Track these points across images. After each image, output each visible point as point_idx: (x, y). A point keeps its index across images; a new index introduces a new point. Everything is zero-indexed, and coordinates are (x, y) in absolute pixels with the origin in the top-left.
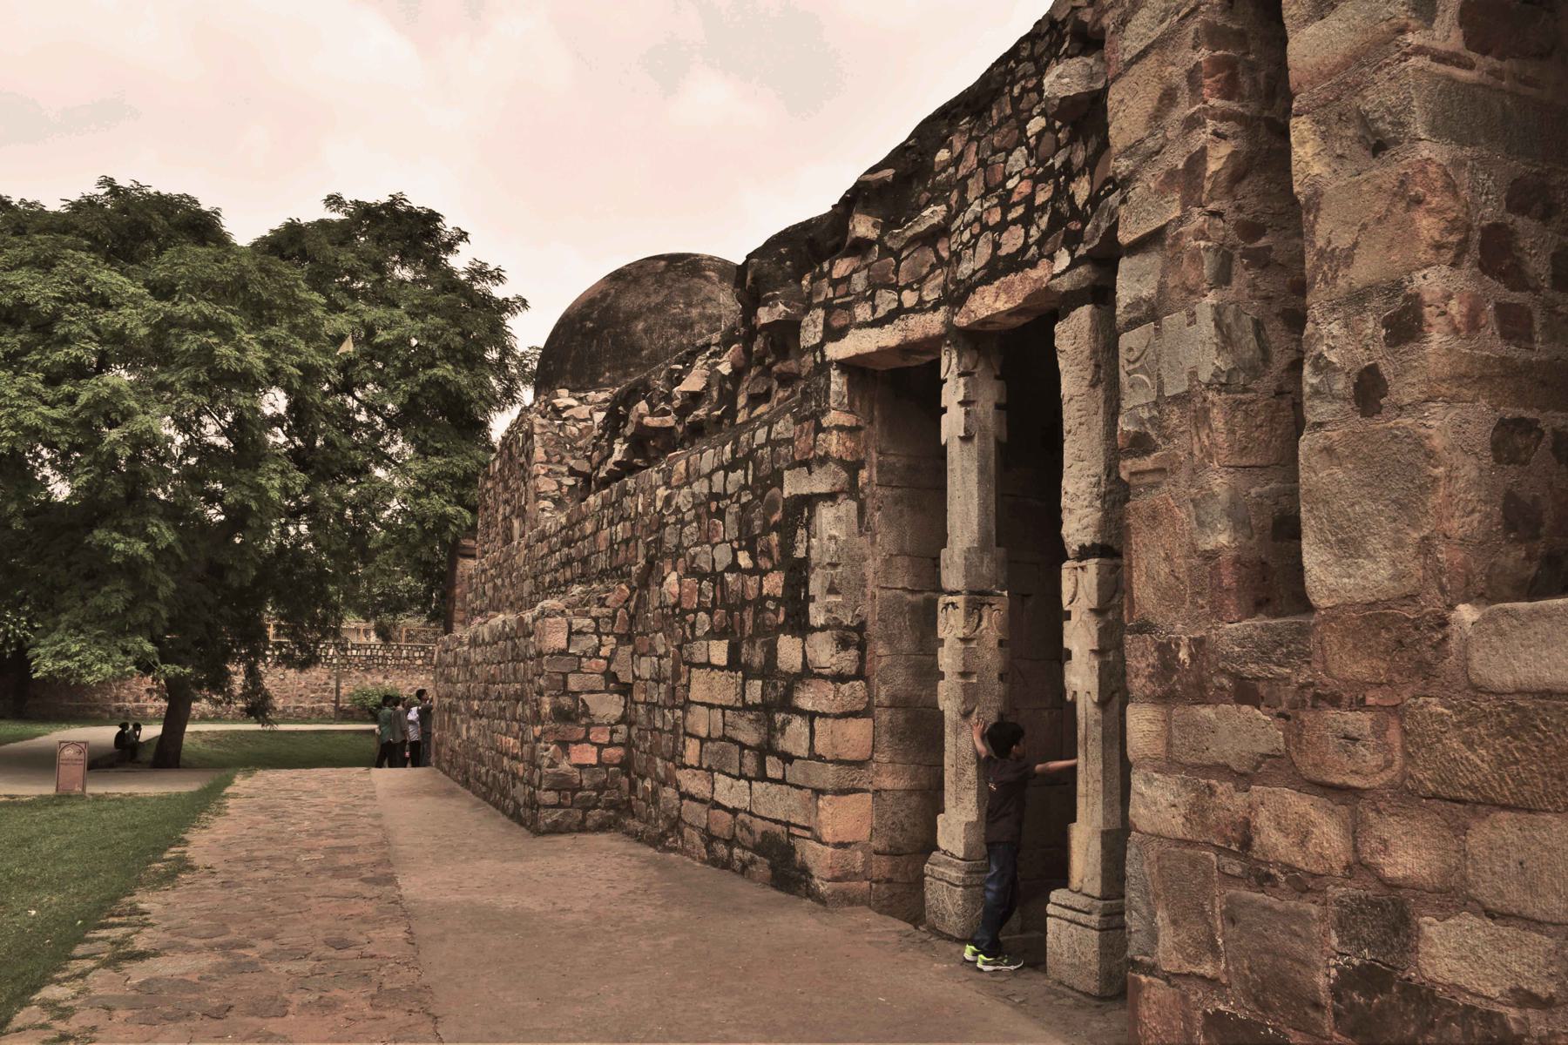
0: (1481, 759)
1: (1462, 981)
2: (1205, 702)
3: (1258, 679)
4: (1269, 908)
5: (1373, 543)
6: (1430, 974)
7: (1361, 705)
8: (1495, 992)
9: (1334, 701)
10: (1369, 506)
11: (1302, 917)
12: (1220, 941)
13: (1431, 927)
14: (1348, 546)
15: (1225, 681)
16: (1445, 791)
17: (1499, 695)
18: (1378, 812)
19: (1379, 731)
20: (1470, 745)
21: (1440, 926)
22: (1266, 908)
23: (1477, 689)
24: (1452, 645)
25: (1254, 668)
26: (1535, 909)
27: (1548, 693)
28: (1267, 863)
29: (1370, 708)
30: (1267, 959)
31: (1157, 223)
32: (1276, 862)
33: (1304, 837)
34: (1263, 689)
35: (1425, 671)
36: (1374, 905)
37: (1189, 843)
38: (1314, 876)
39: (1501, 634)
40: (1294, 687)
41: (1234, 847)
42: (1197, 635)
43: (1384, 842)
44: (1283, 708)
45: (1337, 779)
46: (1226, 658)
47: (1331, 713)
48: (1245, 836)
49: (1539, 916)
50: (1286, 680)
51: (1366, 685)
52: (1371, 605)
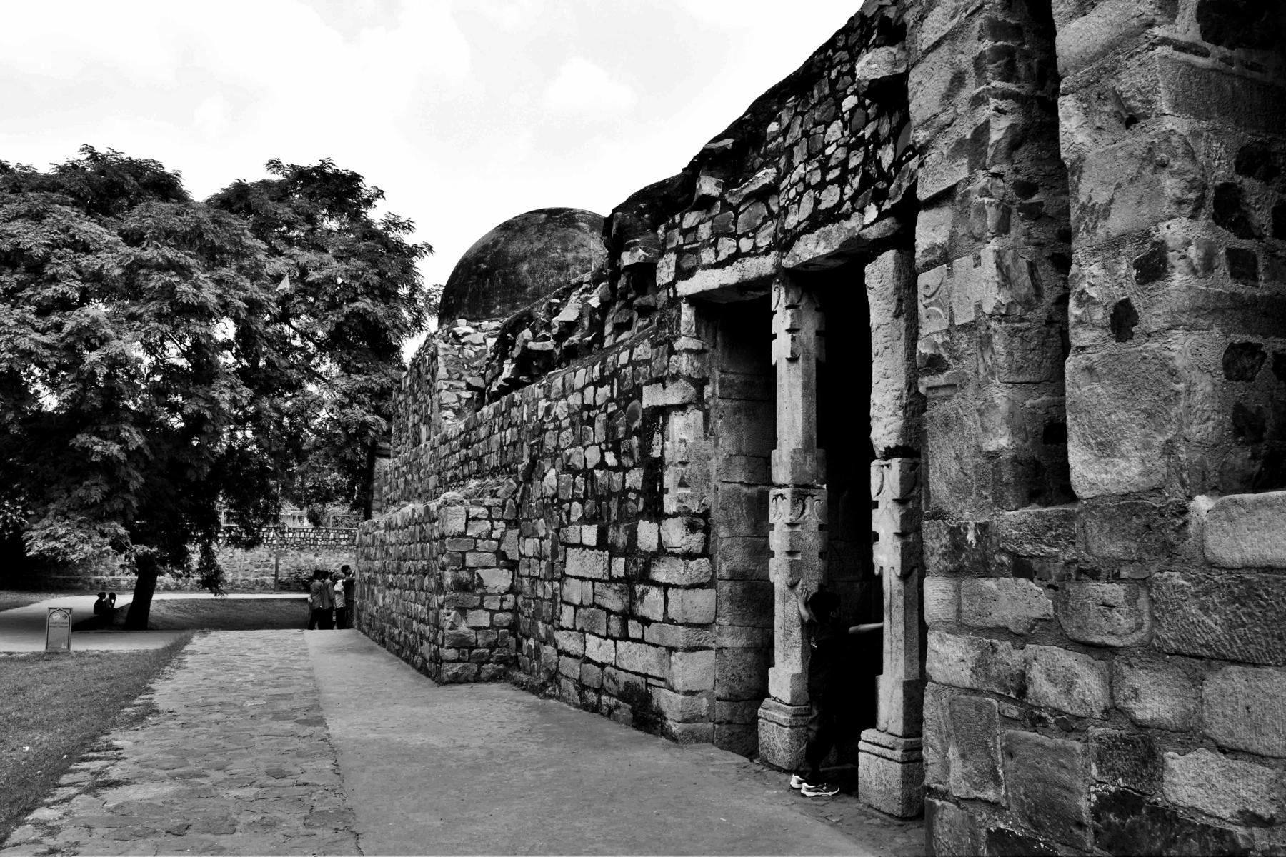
0: (1214, 623)
1: (1198, 805)
2: (988, 575)
3: (1031, 557)
4: (1041, 745)
5: (1126, 446)
6: (1173, 799)
7: (1116, 578)
8: (1226, 814)
9: (1094, 575)
10: (1122, 415)
11: (1067, 752)
12: (1001, 772)
13: (1174, 760)
14: (1105, 448)
15: (1005, 559)
16: (1185, 649)
17: (1230, 570)
18: (1131, 666)
19: (1132, 600)
20: (1205, 609)
21: (1181, 759)
22: (1037, 745)
23: (1211, 565)
24: (1191, 529)
25: (1029, 548)
26: (1258, 745)
27: (1269, 569)
28: (1039, 708)
29: (1123, 581)
30: (1039, 787)
31: (948, 183)
32: (1046, 707)
33: (1069, 686)
34: (1036, 565)
35: (1169, 551)
36: (1127, 742)
37: (975, 692)
38: (1077, 718)
39: (1231, 520)
40: (1061, 563)
41: (1012, 695)
42: (982, 521)
43: (1135, 691)
44: (1052, 581)
45: (1097, 639)
46: (1005, 539)
47: (1092, 586)
48: (1020, 685)
49: (1262, 751)
50: (1055, 557)
51: (1119, 562)
52: (1124, 496)
